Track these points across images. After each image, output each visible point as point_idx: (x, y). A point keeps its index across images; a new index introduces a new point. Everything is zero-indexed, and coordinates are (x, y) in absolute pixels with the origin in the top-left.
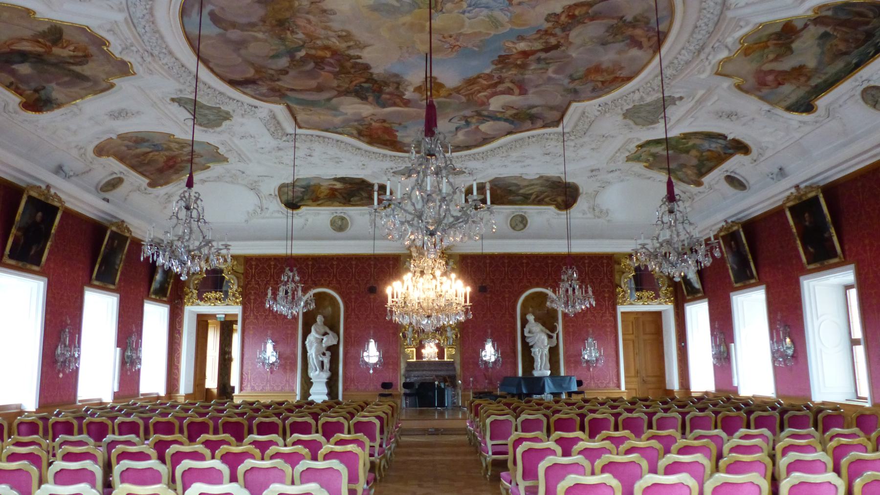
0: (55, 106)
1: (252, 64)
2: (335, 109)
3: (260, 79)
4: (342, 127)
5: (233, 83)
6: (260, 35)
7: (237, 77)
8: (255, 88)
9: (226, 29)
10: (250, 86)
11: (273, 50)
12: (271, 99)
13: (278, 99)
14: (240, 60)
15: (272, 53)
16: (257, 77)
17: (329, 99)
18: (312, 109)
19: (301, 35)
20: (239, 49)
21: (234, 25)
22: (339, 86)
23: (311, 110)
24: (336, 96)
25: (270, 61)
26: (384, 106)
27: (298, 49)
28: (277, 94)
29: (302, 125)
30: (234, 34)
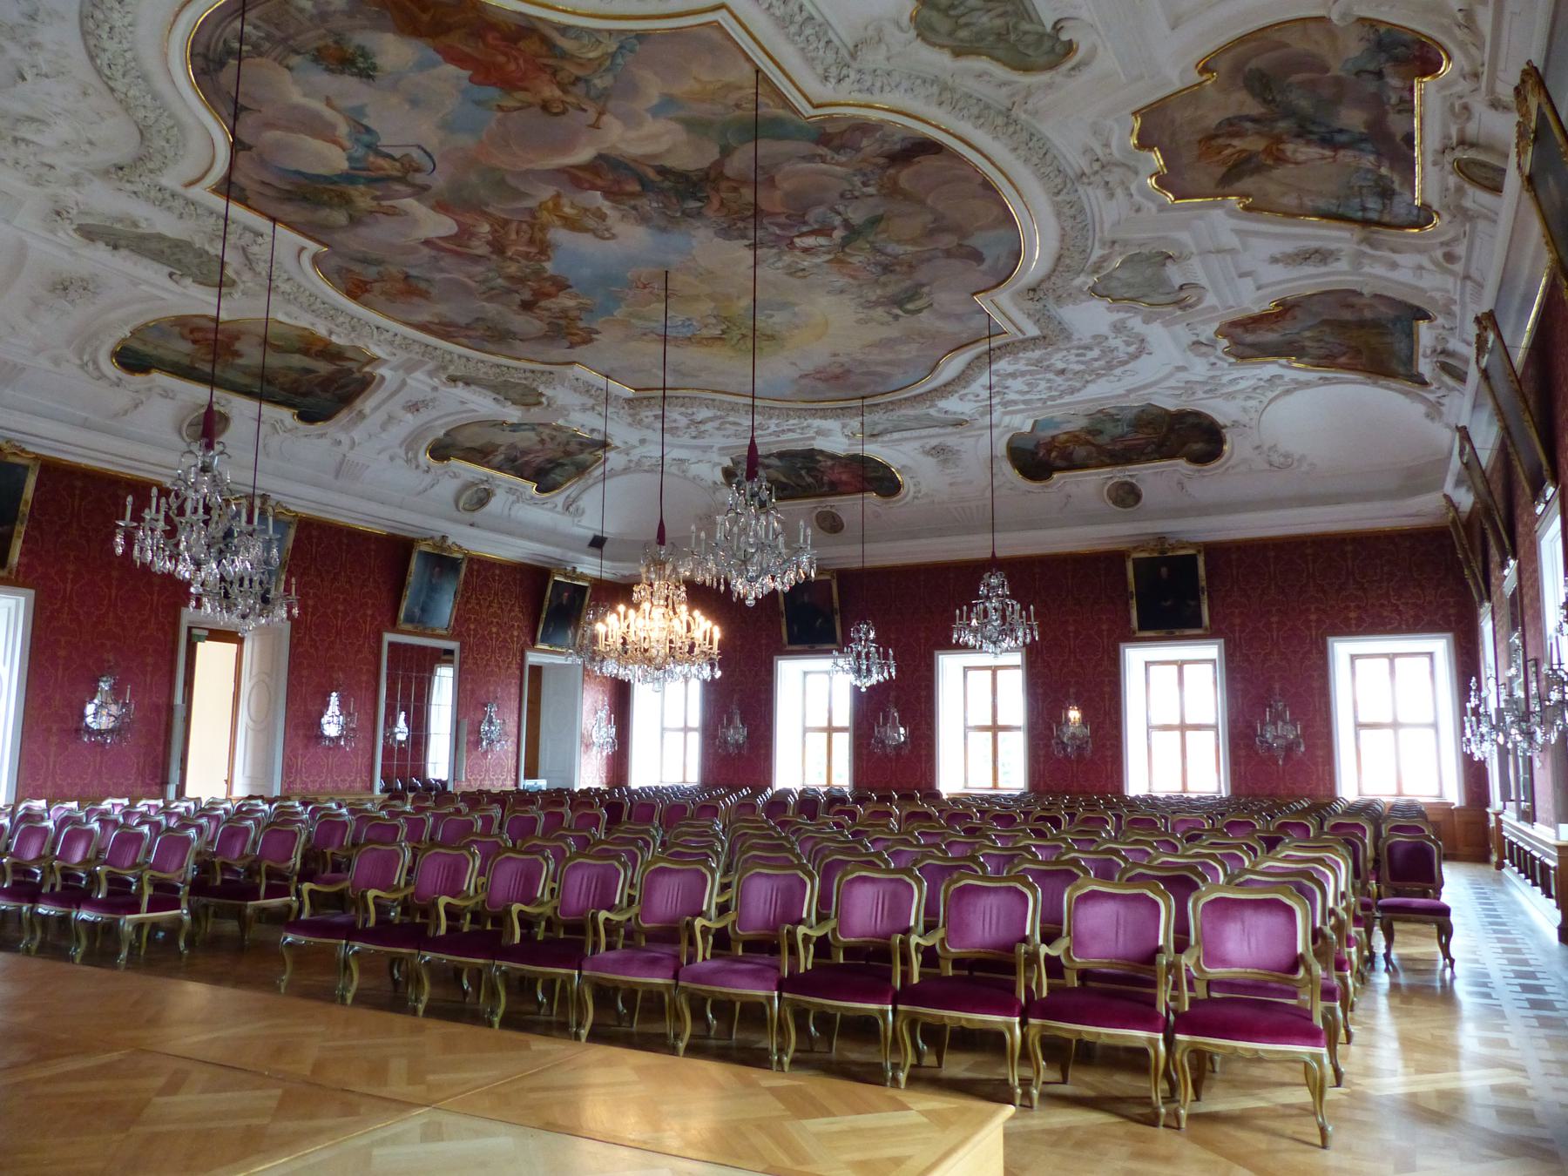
0: (1382, 29)
1: (907, 196)
2: (694, 126)
3: (884, 168)
4: (613, 56)
5: (929, 147)
6: (910, 248)
7: (928, 163)
8: (886, 147)
9: (960, 245)
10: (898, 147)
11: (884, 231)
12: (844, 126)
13: (830, 129)
14: (929, 201)
15: (883, 225)
16: (892, 171)
17: (726, 152)
18: (738, 113)
19: (854, 260)
20: (935, 220)
21: (948, 254)
22: (736, 189)
23: (738, 106)
24: (718, 165)
25: (880, 211)
26: (600, 156)
27: (846, 242)
28: (836, 142)
29: (716, 36)
30: (948, 240)
